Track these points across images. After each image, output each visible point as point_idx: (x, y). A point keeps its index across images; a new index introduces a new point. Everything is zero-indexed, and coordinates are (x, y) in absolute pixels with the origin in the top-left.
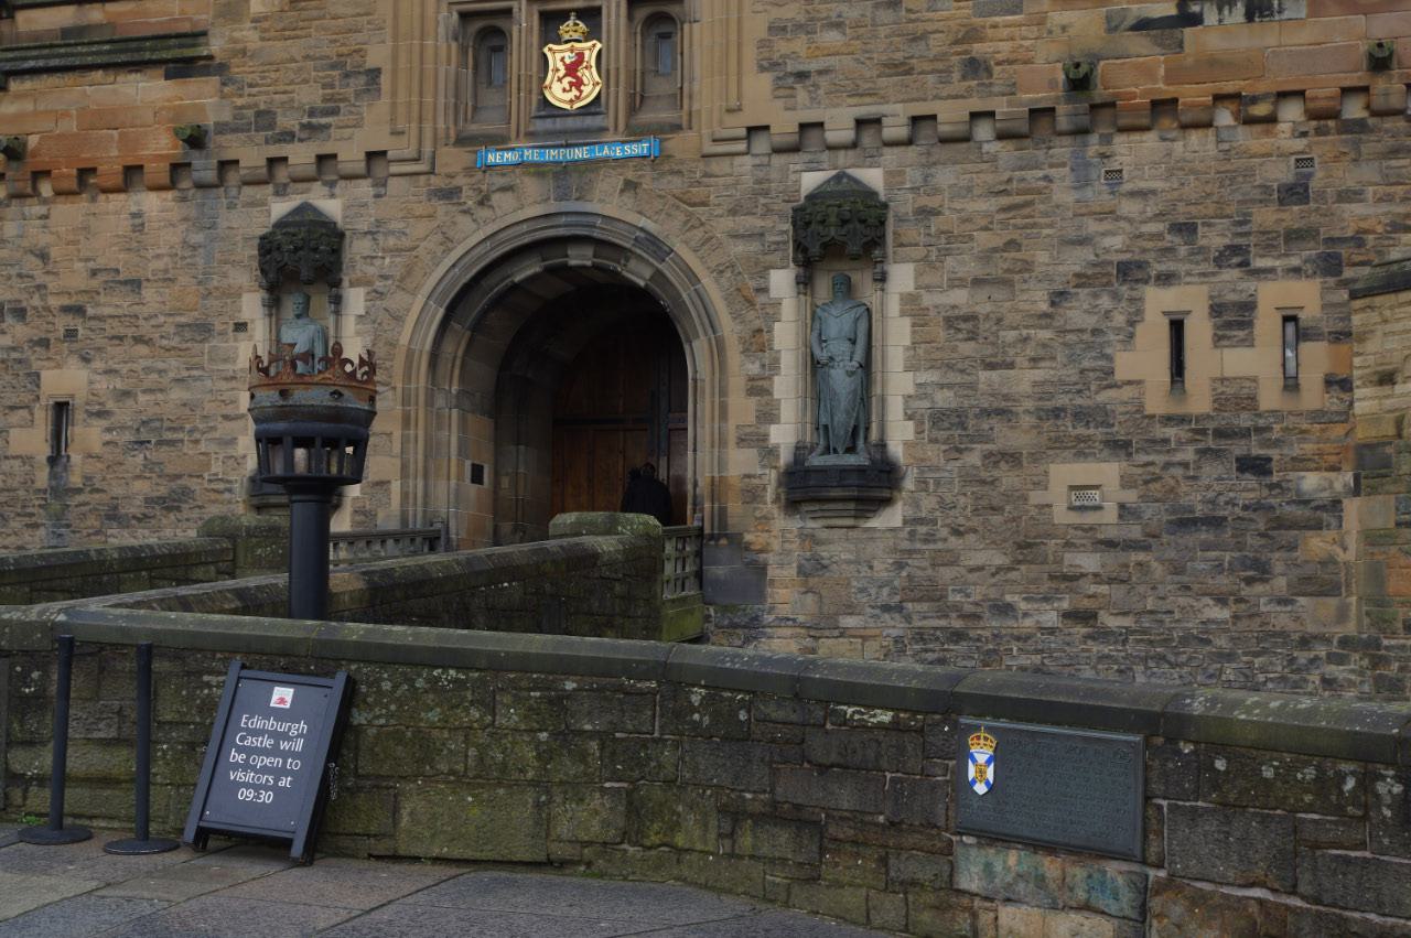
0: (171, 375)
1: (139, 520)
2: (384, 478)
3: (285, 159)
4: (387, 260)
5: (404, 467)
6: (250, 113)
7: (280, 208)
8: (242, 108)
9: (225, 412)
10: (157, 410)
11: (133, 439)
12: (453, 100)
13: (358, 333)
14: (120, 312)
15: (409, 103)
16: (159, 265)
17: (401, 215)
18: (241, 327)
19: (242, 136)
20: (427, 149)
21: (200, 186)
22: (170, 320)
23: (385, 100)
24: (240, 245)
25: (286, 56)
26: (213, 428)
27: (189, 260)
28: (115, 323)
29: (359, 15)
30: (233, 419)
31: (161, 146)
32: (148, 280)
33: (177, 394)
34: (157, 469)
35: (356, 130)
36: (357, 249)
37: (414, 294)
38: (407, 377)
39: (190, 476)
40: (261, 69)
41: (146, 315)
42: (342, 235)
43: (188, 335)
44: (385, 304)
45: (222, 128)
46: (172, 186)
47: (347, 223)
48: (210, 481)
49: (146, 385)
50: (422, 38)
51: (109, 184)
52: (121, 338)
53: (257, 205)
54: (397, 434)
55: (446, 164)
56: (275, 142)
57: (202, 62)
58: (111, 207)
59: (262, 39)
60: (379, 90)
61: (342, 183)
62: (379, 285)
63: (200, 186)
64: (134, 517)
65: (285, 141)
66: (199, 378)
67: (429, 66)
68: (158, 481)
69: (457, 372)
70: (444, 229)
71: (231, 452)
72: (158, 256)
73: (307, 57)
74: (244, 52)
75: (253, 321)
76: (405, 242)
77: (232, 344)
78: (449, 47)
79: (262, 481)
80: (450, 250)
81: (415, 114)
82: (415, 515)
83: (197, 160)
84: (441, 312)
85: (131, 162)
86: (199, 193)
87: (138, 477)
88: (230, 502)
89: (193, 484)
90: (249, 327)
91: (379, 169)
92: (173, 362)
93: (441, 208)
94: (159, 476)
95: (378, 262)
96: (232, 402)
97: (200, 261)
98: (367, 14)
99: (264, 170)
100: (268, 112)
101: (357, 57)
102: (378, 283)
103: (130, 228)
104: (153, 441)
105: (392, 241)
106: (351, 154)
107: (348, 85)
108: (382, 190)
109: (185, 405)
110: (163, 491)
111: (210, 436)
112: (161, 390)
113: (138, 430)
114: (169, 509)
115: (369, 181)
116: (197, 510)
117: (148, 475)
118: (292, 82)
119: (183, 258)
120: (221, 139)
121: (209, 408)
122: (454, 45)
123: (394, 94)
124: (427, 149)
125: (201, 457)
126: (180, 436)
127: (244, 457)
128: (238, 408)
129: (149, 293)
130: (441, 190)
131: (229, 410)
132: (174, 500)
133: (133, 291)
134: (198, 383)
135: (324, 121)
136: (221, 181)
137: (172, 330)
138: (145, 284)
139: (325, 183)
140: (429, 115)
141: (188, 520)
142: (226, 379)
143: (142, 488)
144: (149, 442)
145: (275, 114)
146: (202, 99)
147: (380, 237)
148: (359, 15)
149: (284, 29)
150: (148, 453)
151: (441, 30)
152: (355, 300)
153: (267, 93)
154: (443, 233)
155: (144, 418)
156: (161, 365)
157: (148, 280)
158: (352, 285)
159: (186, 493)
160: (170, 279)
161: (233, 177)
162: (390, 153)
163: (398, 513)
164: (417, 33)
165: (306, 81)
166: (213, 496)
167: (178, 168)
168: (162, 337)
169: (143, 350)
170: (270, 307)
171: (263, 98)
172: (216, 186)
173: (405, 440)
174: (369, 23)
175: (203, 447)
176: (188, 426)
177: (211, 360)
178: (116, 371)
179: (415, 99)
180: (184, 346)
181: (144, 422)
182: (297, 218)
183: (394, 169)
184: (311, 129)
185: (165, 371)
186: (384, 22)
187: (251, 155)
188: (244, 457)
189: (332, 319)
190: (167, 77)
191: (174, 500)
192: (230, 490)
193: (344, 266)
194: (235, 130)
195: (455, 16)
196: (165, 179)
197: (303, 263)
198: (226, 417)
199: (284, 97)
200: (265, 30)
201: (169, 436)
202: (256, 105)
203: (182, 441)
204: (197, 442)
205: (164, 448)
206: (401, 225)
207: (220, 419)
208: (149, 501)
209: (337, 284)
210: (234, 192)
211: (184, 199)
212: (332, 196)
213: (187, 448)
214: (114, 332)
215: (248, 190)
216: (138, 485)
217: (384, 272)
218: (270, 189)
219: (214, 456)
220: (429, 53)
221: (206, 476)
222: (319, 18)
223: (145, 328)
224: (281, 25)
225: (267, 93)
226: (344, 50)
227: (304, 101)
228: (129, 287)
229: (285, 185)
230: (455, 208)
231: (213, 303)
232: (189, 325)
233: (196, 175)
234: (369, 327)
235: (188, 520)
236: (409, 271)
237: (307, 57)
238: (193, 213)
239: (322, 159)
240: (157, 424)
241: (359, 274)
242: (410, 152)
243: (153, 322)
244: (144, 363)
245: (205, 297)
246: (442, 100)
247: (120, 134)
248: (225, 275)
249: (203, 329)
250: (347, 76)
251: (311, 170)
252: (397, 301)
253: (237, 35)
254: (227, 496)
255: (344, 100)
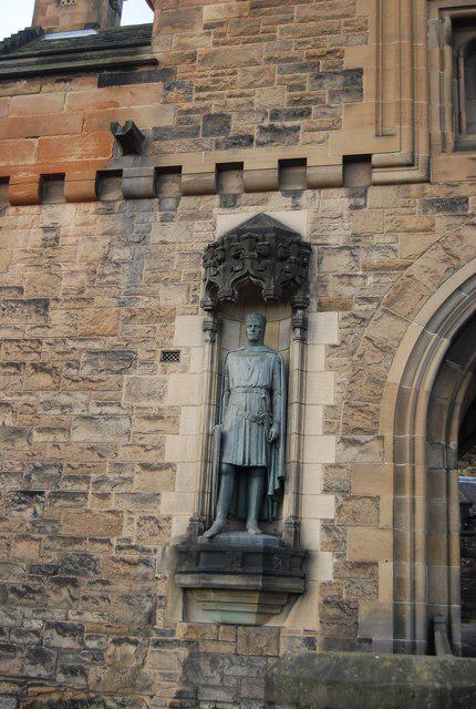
0: (77, 411)
1: (21, 595)
2: (371, 557)
3: (239, 166)
4: (371, 279)
5: (397, 544)
6: (197, 117)
7: (228, 221)
8: (189, 111)
9: (144, 460)
10: (55, 453)
11: (19, 488)
12: (448, 106)
13: (330, 367)
14: (18, 335)
15: (400, 104)
16: (75, 282)
17: (387, 227)
18: (170, 356)
19: (187, 141)
20: (422, 154)
21: (130, 196)
22: (82, 345)
23: (368, 101)
24: (176, 261)
25: (245, 59)
26: (130, 480)
27: (110, 278)
28: (13, 348)
29: (333, 17)
30: (156, 469)
31: (82, 156)
32: (57, 300)
33: (82, 435)
34: (49, 529)
35: (333, 134)
36: (330, 267)
37: (406, 320)
38: (399, 426)
39: (93, 540)
40: (212, 72)
41: (51, 341)
42: (308, 246)
43: (102, 364)
44: (367, 332)
45: (161, 134)
46: (96, 197)
47: (318, 237)
48: (119, 548)
49: (46, 422)
50: (412, 39)
51: (21, 193)
52: (17, 366)
53: (200, 218)
54: (387, 499)
55: (445, 173)
56: (227, 147)
57: (145, 69)
58: (21, 220)
59: (216, 44)
60: (361, 91)
61: (309, 193)
62: (357, 308)
63: (130, 196)
64: (14, 590)
65: (240, 144)
66: (114, 417)
67: (421, 68)
68: (49, 544)
69: (456, 424)
70: (447, 245)
71: (149, 511)
72: (72, 273)
73: (269, 59)
74: (193, 57)
75: (188, 349)
76: (393, 259)
77: (159, 376)
78: (442, 52)
79: (187, 555)
80: (456, 269)
81: (407, 115)
82: (414, 612)
83: (127, 164)
84: (445, 343)
85: (50, 170)
86: (129, 204)
87: (24, 537)
88: (145, 578)
89: (97, 551)
90: (182, 356)
91: (359, 176)
92: (81, 396)
93: (441, 221)
94: (51, 538)
95: (359, 281)
96: (155, 448)
97: (124, 280)
98: (347, 16)
99: (213, 177)
100: (221, 115)
101: (332, 60)
102: (356, 307)
103: (41, 243)
104: (47, 493)
105: (375, 258)
106: (324, 157)
107: (320, 86)
108: (361, 201)
109: (92, 449)
110: (53, 558)
111: (123, 489)
112: (63, 430)
113: (28, 478)
114: (61, 582)
115: (343, 191)
116: (100, 587)
117: (36, 536)
118: (251, 85)
119: (104, 275)
120: (157, 143)
121: (124, 454)
122: (447, 49)
123: (379, 93)
124: (422, 154)
125: (110, 516)
126: (84, 487)
127: (169, 519)
128: (162, 455)
129: (57, 316)
130: (439, 200)
131: (151, 457)
132: (69, 572)
133: (37, 312)
134: (111, 423)
135: (289, 124)
136: (155, 193)
137: (83, 357)
138: (52, 304)
139: (287, 194)
140: (421, 117)
141: (85, 598)
142: (149, 418)
143: (25, 550)
144: (41, 493)
145: (230, 117)
146: (143, 106)
147: (362, 256)
148: (333, 17)
149: (241, 34)
150: (38, 508)
151: (433, 34)
152: (327, 326)
153: (221, 97)
154: (445, 249)
155: (38, 464)
156: (64, 399)
157: (57, 300)
158: (322, 308)
159: (86, 562)
160: (84, 299)
161: (171, 187)
162: (374, 157)
163: (391, 609)
164: (406, 32)
165: (269, 83)
166: (123, 569)
167: (105, 176)
168: (69, 366)
169: (44, 380)
170: (213, 331)
171: (215, 102)
172: (149, 197)
173: (397, 507)
174: (346, 24)
175: (112, 504)
176: (94, 477)
177: (129, 393)
178: (7, 405)
179: (406, 99)
180: (95, 378)
181: (36, 468)
182: (256, 226)
183: (378, 176)
184: (275, 133)
185: (69, 406)
186: (366, 22)
187: (198, 162)
188: (169, 519)
189: (296, 347)
190: (100, 85)
191: (69, 572)
192: (146, 563)
193: (311, 286)
194: (181, 135)
195: (448, 21)
196: (89, 187)
197: (263, 281)
198: (146, 467)
199: (241, 100)
200: (221, 35)
201: (69, 487)
202: (206, 108)
203: (85, 494)
204: (105, 496)
205: (61, 502)
206: (388, 239)
207: (138, 469)
208: (36, 570)
209: (305, 306)
210: (170, 203)
211: (109, 212)
212: (296, 207)
213: (92, 504)
214: (10, 359)
215: (186, 202)
216: (25, 550)
217: (366, 293)
218: (216, 199)
219: (126, 516)
220: (421, 54)
221: (114, 541)
222: (286, 21)
223: (48, 354)
224: (240, 30)
225: (221, 97)
226: (317, 52)
227: (265, 103)
228: (33, 307)
229: (235, 197)
230: (459, 221)
231: (141, 328)
232: (104, 352)
233: (126, 183)
234: (345, 360)
235: (85, 598)
236: (400, 293)
237: (269, 59)
238: (119, 227)
239: (284, 164)
240: (54, 471)
241: (331, 295)
242: (402, 156)
243: (60, 348)
244: (43, 397)
245: (127, 320)
246: (436, 104)
247: (40, 142)
248: (154, 295)
249: (124, 358)
250: (319, 77)
251: (273, 176)
252: (381, 329)
253: (189, 41)
254: (142, 569)
255: (316, 101)
